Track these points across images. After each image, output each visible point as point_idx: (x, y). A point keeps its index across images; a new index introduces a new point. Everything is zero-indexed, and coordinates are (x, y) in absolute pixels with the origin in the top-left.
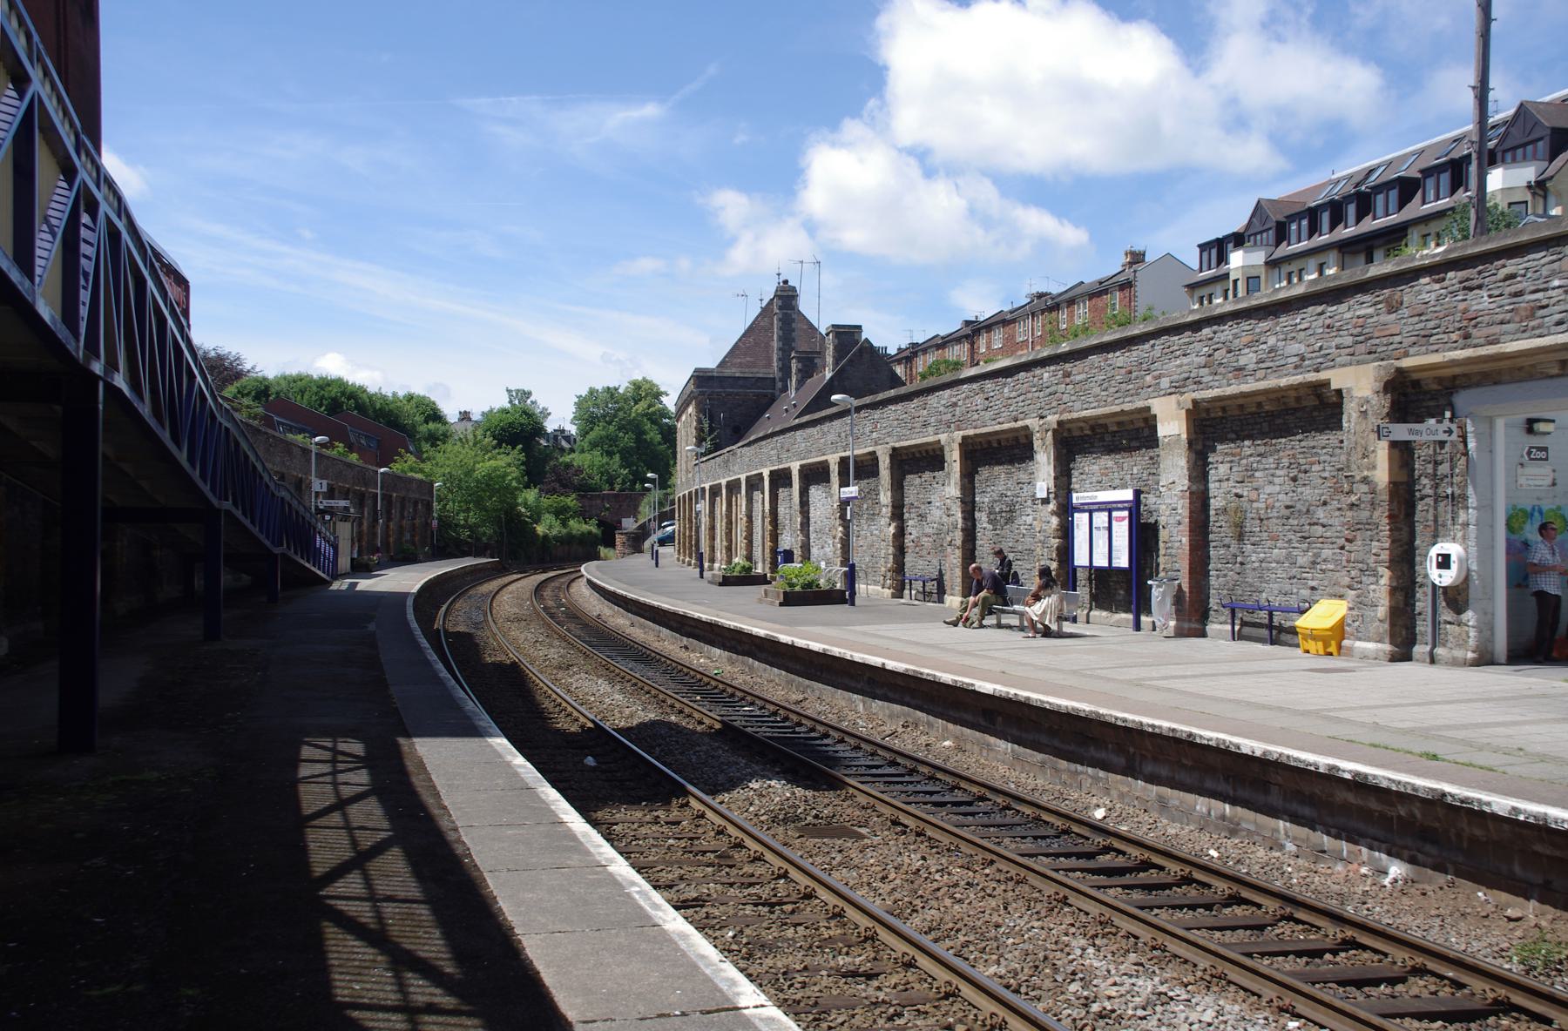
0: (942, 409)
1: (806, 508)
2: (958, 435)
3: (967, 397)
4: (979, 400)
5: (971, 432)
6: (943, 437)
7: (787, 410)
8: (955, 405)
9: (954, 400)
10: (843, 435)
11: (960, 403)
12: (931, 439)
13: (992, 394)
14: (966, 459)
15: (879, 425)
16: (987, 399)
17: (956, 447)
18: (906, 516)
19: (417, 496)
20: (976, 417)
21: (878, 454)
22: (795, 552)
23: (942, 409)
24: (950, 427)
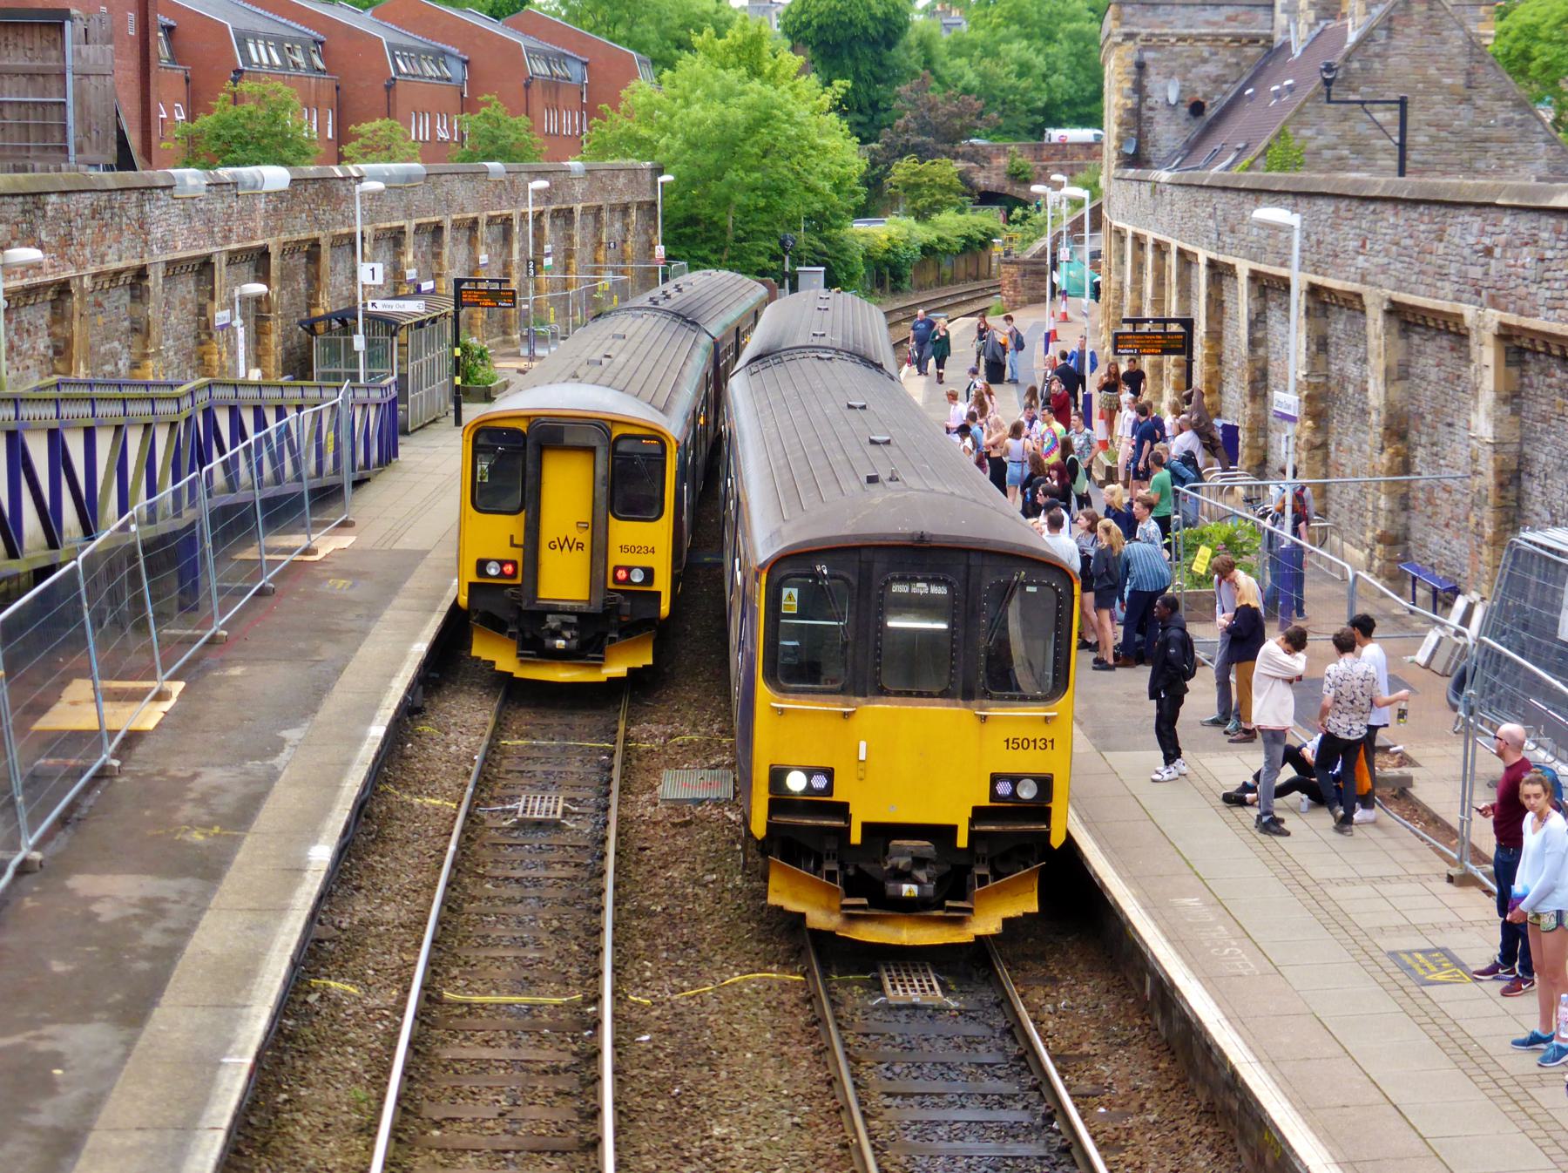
0: (1467, 252)
1: (1261, 351)
2: (1494, 317)
3: (1508, 245)
4: (1527, 256)
5: (1512, 319)
6: (1469, 312)
7: (1278, 95)
8: (1488, 252)
9: (1487, 241)
10: (1313, 238)
11: (1497, 252)
12: (1446, 306)
13: (1549, 254)
14: (1508, 363)
15: (1368, 246)
16: (1542, 260)
17: (1488, 336)
18: (1413, 436)
19: (627, 199)
20: (1522, 291)
21: (1367, 300)
22: (1241, 435)
23: (1467, 252)
24: (1478, 293)
